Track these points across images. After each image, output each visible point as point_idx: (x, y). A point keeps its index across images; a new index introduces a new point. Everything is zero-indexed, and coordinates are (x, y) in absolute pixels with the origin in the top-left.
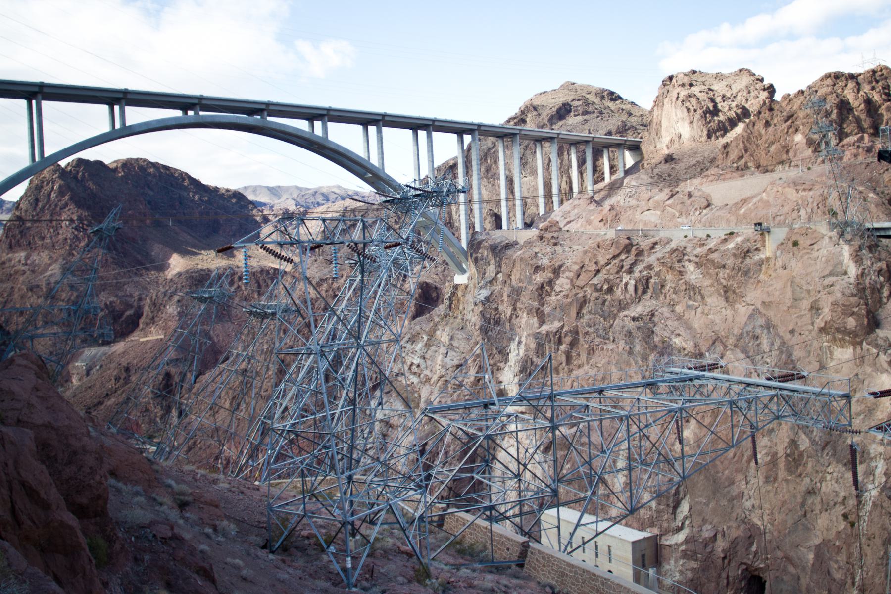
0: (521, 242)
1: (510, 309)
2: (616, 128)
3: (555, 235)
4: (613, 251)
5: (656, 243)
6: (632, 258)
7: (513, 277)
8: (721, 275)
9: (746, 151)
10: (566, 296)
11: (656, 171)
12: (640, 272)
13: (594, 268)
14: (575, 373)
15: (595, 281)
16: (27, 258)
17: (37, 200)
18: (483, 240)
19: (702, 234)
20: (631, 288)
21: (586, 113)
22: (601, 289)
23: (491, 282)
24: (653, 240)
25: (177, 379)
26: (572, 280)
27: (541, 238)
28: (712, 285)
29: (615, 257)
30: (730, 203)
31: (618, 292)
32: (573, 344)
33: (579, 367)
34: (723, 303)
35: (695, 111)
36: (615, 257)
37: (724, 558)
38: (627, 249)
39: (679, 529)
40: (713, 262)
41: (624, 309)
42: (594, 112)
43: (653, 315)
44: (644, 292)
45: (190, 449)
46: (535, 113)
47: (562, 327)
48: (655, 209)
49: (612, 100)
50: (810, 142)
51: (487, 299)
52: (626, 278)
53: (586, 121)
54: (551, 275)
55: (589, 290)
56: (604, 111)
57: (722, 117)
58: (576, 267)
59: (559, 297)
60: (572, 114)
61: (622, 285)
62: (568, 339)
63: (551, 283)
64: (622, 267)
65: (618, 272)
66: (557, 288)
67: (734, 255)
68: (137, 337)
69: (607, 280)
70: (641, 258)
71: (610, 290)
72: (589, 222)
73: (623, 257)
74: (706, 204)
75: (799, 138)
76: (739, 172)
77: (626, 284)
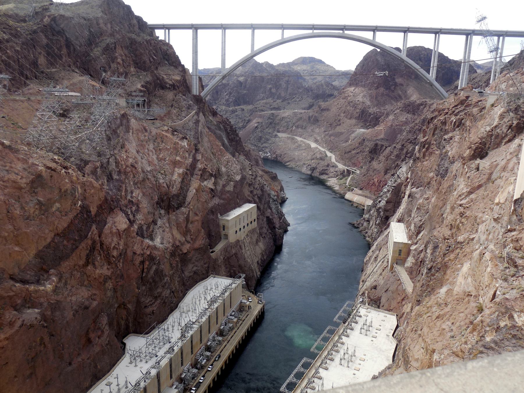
4: (456, 104)
6: (463, 108)
12: (460, 116)
14: (425, 163)
16: (354, 90)
17: (363, 65)
25: (379, 147)
32: (428, 149)
33: (427, 160)
37: (421, 262)
39: (416, 244)
43: (451, 139)
44: (458, 127)
45: (364, 175)
47: (427, 139)
52: (453, 119)
62: (426, 146)
64: (454, 112)
65: (450, 114)
68: (376, 128)
77: (452, 121)
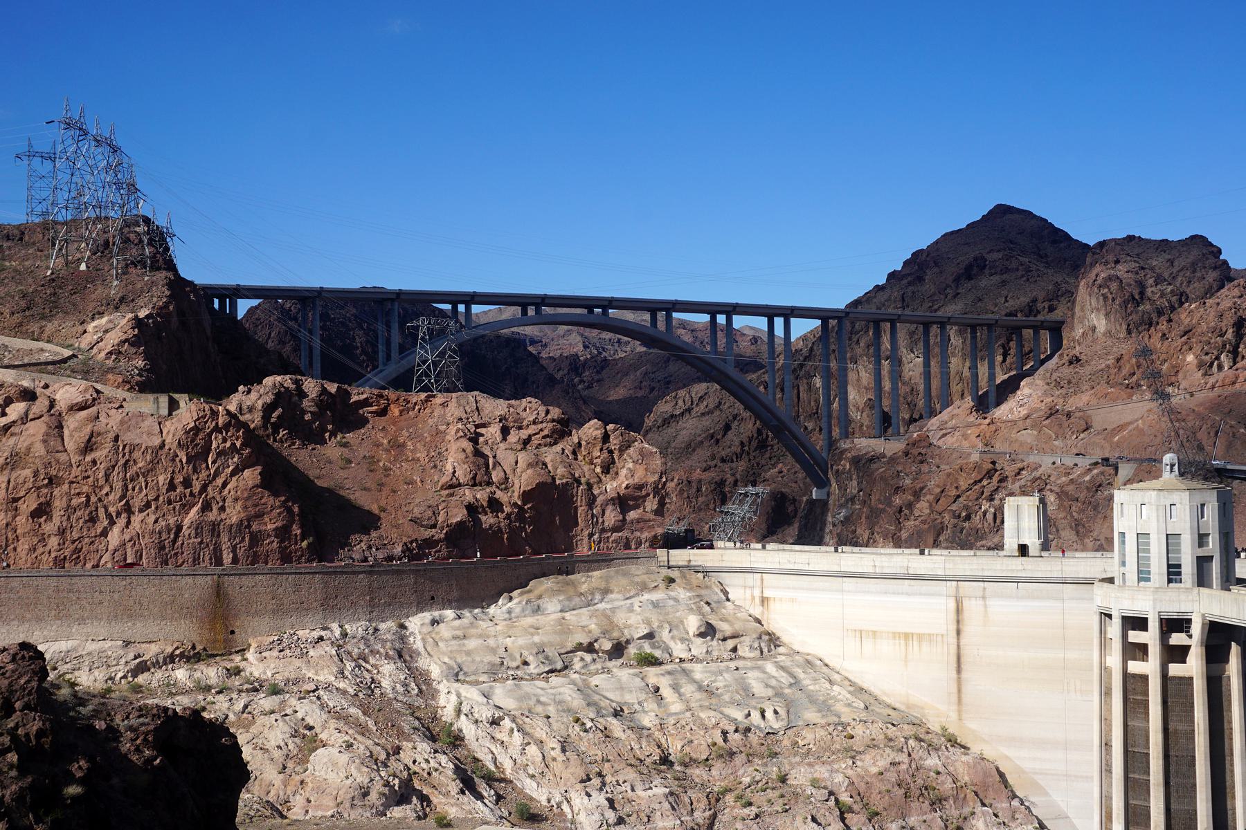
0: (889, 454)
1: (867, 532)
2: (1043, 294)
3: (923, 451)
4: (975, 476)
5: (1023, 469)
7: (872, 497)
8: (1073, 508)
9: (1138, 367)
10: (924, 522)
11: (1055, 375)
13: (954, 492)
15: (954, 507)
18: (846, 450)
19: (1069, 461)
20: (990, 516)
21: (1006, 270)
22: (959, 516)
23: (852, 500)
24: (1020, 465)
26: (931, 506)
27: (906, 454)
28: (1065, 518)
29: (975, 483)
30: (1110, 428)
31: (976, 519)
34: (1075, 538)
35: (1114, 299)
36: (975, 483)
38: (989, 474)
40: (1066, 494)
41: (982, 539)
42: (1017, 270)
46: (936, 270)
48: (1033, 427)
49: (1054, 242)
50: (1200, 365)
51: (847, 519)
53: (1004, 283)
54: (911, 498)
55: (947, 516)
56: (1033, 267)
57: (1146, 307)
58: (938, 490)
59: (917, 523)
60: (987, 271)
61: (980, 513)
63: (910, 506)
65: (977, 499)
66: (917, 513)
67: (1087, 488)
69: (966, 507)
70: (1003, 484)
71: (968, 518)
72: (965, 436)
73: (985, 482)
74: (1084, 427)
75: (1190, 358)
76: (1129, 390)
77: (985, 513)
